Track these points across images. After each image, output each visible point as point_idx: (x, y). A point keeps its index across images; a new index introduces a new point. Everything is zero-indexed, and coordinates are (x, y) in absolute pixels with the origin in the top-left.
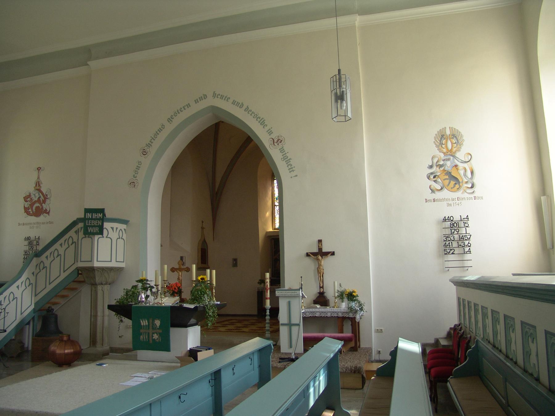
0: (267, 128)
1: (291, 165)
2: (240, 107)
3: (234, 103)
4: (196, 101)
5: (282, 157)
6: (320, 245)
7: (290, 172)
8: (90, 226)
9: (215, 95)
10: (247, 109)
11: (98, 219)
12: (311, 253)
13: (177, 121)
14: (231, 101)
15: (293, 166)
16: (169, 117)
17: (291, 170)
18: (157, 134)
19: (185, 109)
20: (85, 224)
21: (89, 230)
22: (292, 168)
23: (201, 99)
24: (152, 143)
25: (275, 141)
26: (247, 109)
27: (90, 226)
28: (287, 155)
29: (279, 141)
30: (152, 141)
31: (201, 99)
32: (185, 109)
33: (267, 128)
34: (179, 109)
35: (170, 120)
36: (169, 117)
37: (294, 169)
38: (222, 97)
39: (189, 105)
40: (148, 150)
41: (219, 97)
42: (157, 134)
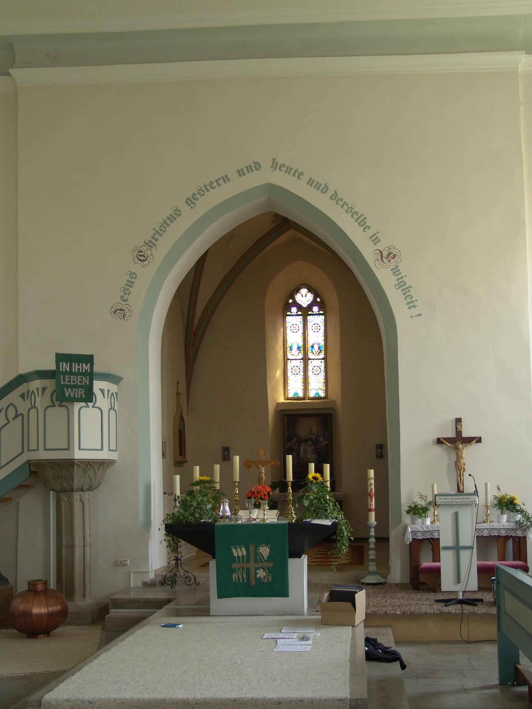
0: (370, 232)
1: (412, 297)
2: (322, 191)
3: (310, 182)
4: (241, 173)
5: (397, 283)
6: (459, 427)
7: (409, 308)
8: (68, 386)
9: (275, 165)
10: (334, 196)
11: (82, 374)
12: (446, 439)
13: (205, 205)
14: (305, 178)
15: (414, 299)
16: (190, 196)
17: (411, 305)
18: (165, 225)
19: (219, 185)
20: (58, 383)
21: (68, 393)
22: (413, 302)
23: (249, 169)
24: (157, 240)
25: (385, 254)
26: (334, 196)
27: (68, 386)
28: (405, 279)
29: (391, 256)
30: (157, 236)
31: (249, 169)
32: (219, 185)
33: (370, 232)
34: (207, 183)
35: (191, 201)
36: (190, 196)
37: (415, 303)
38: (288, 170)
39: (226, 179)
40: (149, 252)
41: (284, 169)
42: (165, 225)
